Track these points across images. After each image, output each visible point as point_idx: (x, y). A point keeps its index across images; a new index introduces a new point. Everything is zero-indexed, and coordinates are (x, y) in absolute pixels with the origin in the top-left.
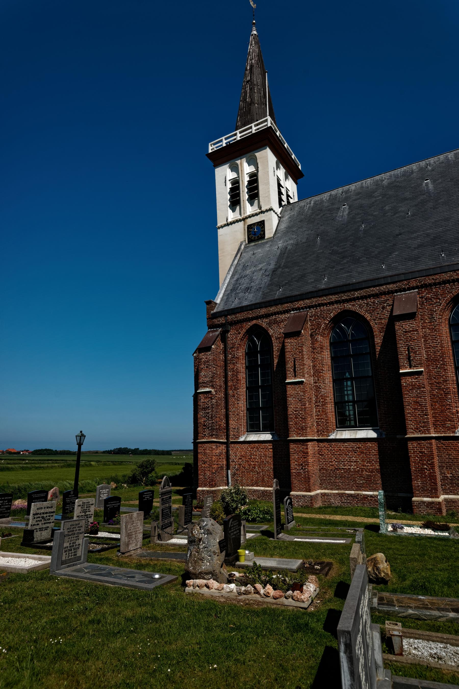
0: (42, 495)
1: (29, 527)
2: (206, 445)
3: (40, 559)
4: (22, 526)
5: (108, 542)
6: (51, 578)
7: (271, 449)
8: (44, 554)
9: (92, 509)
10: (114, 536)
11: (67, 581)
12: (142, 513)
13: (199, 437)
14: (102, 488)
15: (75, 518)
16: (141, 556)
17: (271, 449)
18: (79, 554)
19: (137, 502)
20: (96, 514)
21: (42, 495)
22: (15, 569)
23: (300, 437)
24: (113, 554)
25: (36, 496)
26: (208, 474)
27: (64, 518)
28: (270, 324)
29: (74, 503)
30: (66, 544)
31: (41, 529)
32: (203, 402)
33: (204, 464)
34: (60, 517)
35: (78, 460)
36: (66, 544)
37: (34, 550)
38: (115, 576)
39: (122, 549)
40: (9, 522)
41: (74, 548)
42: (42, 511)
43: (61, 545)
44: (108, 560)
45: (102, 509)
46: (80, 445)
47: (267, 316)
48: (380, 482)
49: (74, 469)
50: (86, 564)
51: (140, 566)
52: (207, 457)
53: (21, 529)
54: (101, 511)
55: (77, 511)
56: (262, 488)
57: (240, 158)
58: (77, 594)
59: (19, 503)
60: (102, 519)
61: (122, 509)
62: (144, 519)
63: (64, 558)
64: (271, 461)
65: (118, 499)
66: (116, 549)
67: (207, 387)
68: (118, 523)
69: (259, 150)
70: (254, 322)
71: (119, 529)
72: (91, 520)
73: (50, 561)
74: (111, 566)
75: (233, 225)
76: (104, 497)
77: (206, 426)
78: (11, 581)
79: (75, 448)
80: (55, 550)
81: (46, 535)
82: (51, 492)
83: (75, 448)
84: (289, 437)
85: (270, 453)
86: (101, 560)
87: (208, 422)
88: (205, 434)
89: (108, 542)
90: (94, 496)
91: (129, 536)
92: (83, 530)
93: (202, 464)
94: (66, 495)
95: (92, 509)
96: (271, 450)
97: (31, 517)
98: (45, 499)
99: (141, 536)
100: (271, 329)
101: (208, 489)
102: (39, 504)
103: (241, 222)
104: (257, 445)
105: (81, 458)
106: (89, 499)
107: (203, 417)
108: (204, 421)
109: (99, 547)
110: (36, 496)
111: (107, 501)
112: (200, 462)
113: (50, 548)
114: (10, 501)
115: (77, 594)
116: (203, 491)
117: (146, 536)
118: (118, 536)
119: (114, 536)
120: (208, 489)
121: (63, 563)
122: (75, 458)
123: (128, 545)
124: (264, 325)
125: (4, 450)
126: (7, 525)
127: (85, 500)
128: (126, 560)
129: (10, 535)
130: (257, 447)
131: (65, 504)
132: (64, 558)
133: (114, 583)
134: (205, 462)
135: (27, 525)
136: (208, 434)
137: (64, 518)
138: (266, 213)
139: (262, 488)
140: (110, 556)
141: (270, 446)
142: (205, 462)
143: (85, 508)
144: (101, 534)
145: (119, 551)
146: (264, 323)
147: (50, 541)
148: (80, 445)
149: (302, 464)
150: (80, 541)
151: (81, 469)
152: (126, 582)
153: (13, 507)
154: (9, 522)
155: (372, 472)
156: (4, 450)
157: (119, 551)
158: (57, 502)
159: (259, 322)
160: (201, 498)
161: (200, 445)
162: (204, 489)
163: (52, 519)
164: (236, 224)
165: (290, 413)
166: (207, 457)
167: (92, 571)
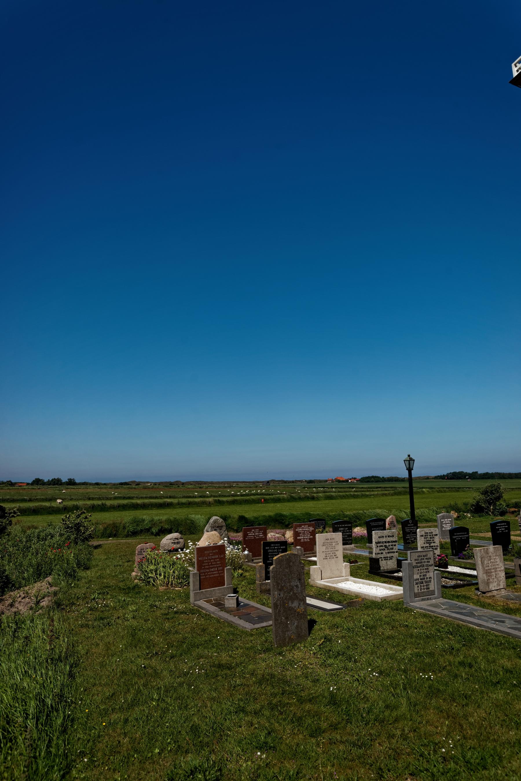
0: (380, 523)
1: (374, 556)
3: (391, 589)
4: (365, 553)
5: (462, 577)
6: (407, 610)
8: (394, 584)
9: (437, 540)
10: (468, 572)
11: (425, 616)
12: (500, 547)
14: (443, 517)
15: (419, 549)
16: (508, 598)
18: (432, 588)
19: (489, 535)
20: (442, 546)
21: (380, 523)
22: (369, 596)
24: (471, 592)
25: (373, 524)
27: (406, 548)
29: (416, 533)
30: (416, 576)
31: (386, 558)
34: (402, 547)
35: (411, 487)
36: (416, 576)
37: (383, 579)
38: (479, 617)
39: (482, 587)
40: (352, 550)
41: (424, 581)
42: (384, 540)
43: (411, 576)
44: (466, 598)
45: (448, 540)
46: (410, 470)
49: (408, 496)
50: (442, 600)
51: (508, 610)
53: (366, 557)
54: (446, 543)
55: (420, 542)
58: (439, 631)
59: (359, 531)
60: (449, 551)
61: (472, 542)
62: (504, 555)
63: (416, 591)
65: (465, 530)
66: (473, 588)
68: (471, 556)
71: (474, 565)
72: (438, 552)
73: (402, 592)
74: (471, 606)
76: (448, 527)
78: (367, 608)
79: (405, 474)
80: (405, 581)
81: (391, 565)
82: (388, 520)
83: (405, 474)
86: (458, 597)
89: (462, 577)
90: (436, 526)
91: (488, 573)
92: (432, 562)
94: (404, 524)
95: (437, 540)
97: (374, 545)
98: (384, 529)
99: (503, 575)
102: (380, 533)
105: (414, 485)
106: (432, 530)
109: (453, 583)
110: (373, 524)
111: (452, 532)
113: (400, 579)
114: (350, 528)
115: (439, 631)
117: (509, 575)
118: (474, 573)
119: (468, 572)
121: (416, 595)
122: (407, 485)
123: (488, 583)
125: (334, 479)
126: (352, 552)
127: (427, 530)
128: (490, 601)
129: (356, 562)
131: (405, 533)
132: (416, 591)
133: (479, 625)
135: (371, 553)
137: (406, 548)
140: (468, 594)
143: (429, 538)
144: (451, 569)
145: (478, 589)
147: (398, 571)
148: (410, 470)
150: (431, 574)
151: (415, 496)
152: (494, 626)
153: (353, 534)
154: (352, 550)
156: (334, 479)
157: (478, 589)
158: (396, 531)
163: (396, 549)
167: (451, 608)
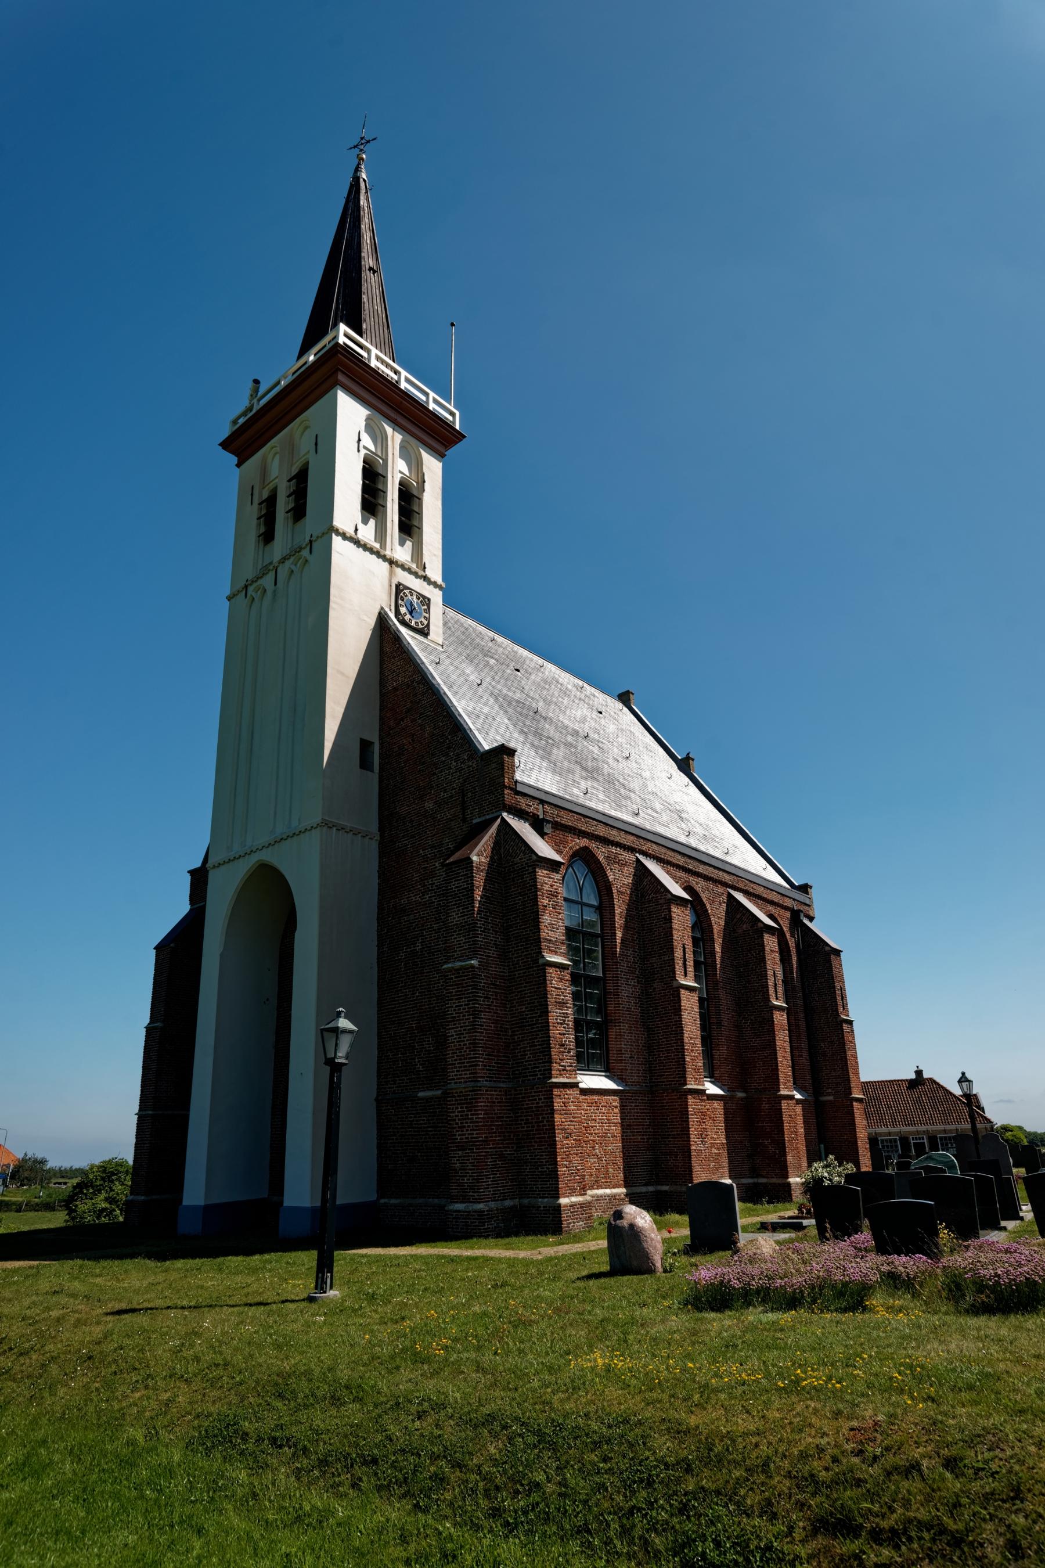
2: (568, 1092)
7: (616, 1107)
13: (553, 1072)
17: (616, 1107)
23: (697, 1085)
26: (576, 1160)
28: (612, 859)
32: (556, 988)
33: (567, 1138)
47: (606, 841)
48: (726, 1164)
52: (571, 1121)
56: (608, 1191)
57: (393, 425)
64: (616, 1130)
67: (556, 953)
69: (432, 452)
70: (584, 842)
75: (367, 553)
77: (563, 1045)
84: (686, 1084)
85: (616, 1116)
87: (567, 1038)
88: (564, 1066)
93: (563, 1137)
96: (617, 1110)
100: (611, 869)
101: (580, 1199)
103: (384, 561)
104: (595, 1097)
107: (558, 1023)
108: (560, 1034)
112: (559, 1133)
116: (573, 1205)
120: (580, 1199)
124: (601, 858)
130: (596, 1103)
134: (568, 1135)
136: (569, 1066)
138: (432, 586)
139: (608, 1191)
141: (615, 1100)
142: (568, 1135)
146: (601, 853)
149: (701, 1135)
155: (718, 1149)
159: (593, 845)
160: (570, 1223)
161: (556, 1092)
162: (574, 1199)
164: (374, 557)
165: (686, 1040)
166: (571, 1121)
